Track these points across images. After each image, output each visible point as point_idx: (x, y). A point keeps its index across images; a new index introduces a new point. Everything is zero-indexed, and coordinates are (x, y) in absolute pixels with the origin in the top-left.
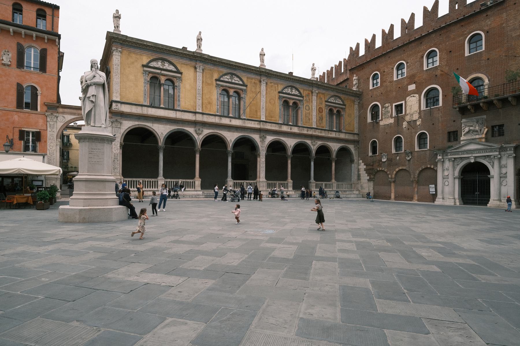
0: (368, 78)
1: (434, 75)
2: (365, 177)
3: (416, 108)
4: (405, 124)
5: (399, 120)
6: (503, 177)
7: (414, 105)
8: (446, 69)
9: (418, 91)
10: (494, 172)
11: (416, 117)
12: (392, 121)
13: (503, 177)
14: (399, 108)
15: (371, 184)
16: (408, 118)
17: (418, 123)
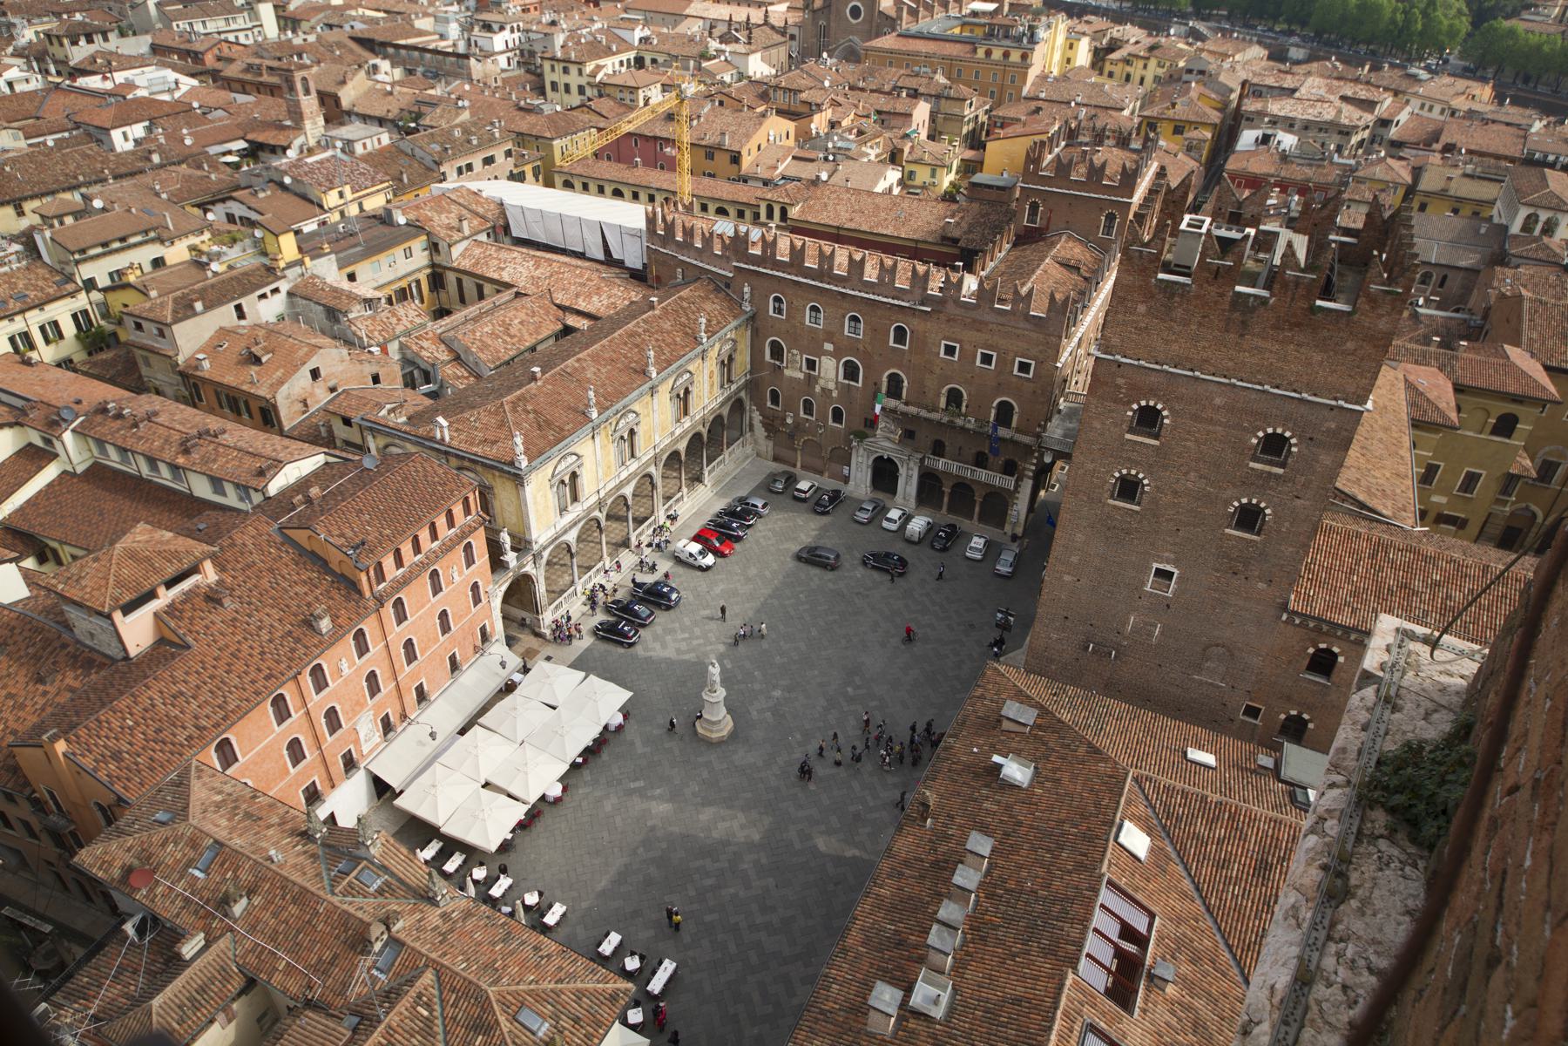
0: (768, 297)
1: (852, 346)
2: (760, 431)
3: (832, 375)
4: (818, 389)
5: (811, 381)
6: (909, 477)
7: (830, 370)
8: (869, 349)
9: (836, 355)
10: (902, 471)
11: (831, 386)
12: (801, 376)
13: (909, 477)
14: (811, 365)
15: (771, 444)
16: (821, 382)
17: (835, 394)
